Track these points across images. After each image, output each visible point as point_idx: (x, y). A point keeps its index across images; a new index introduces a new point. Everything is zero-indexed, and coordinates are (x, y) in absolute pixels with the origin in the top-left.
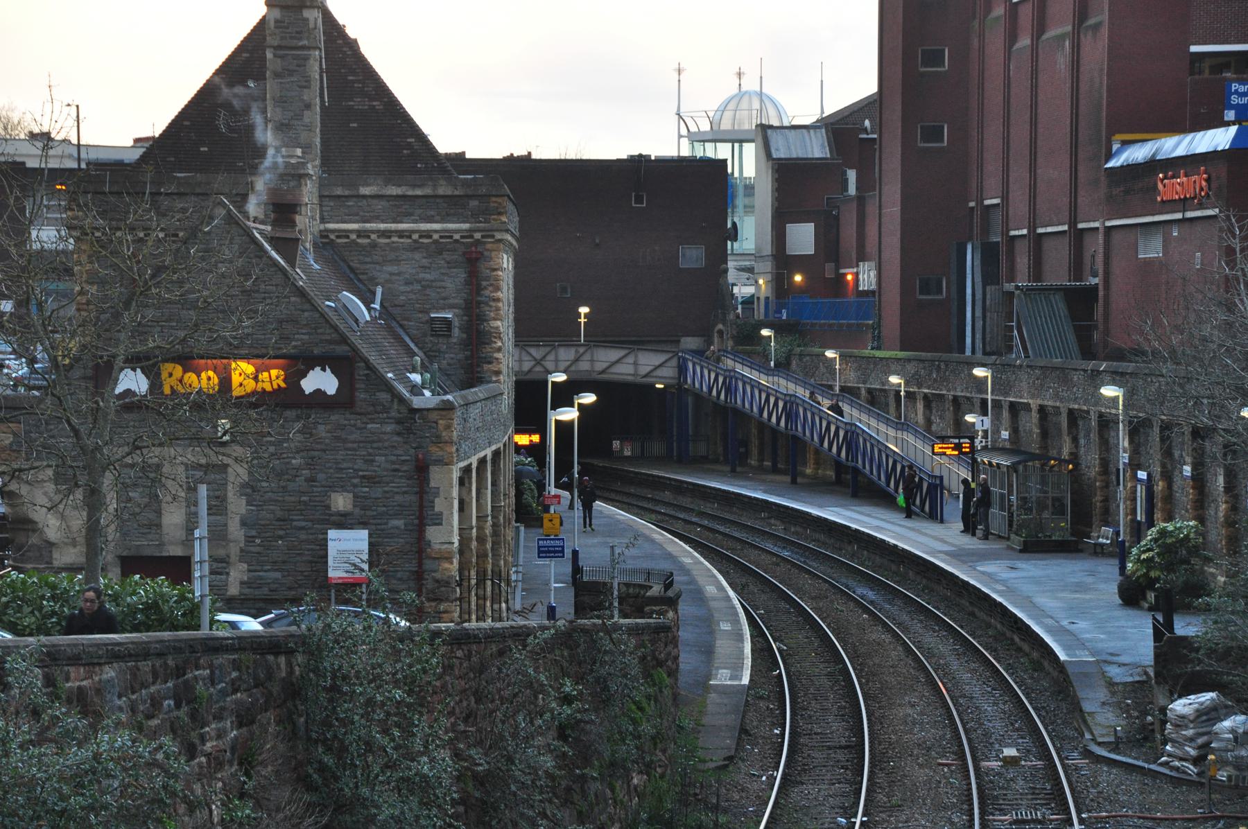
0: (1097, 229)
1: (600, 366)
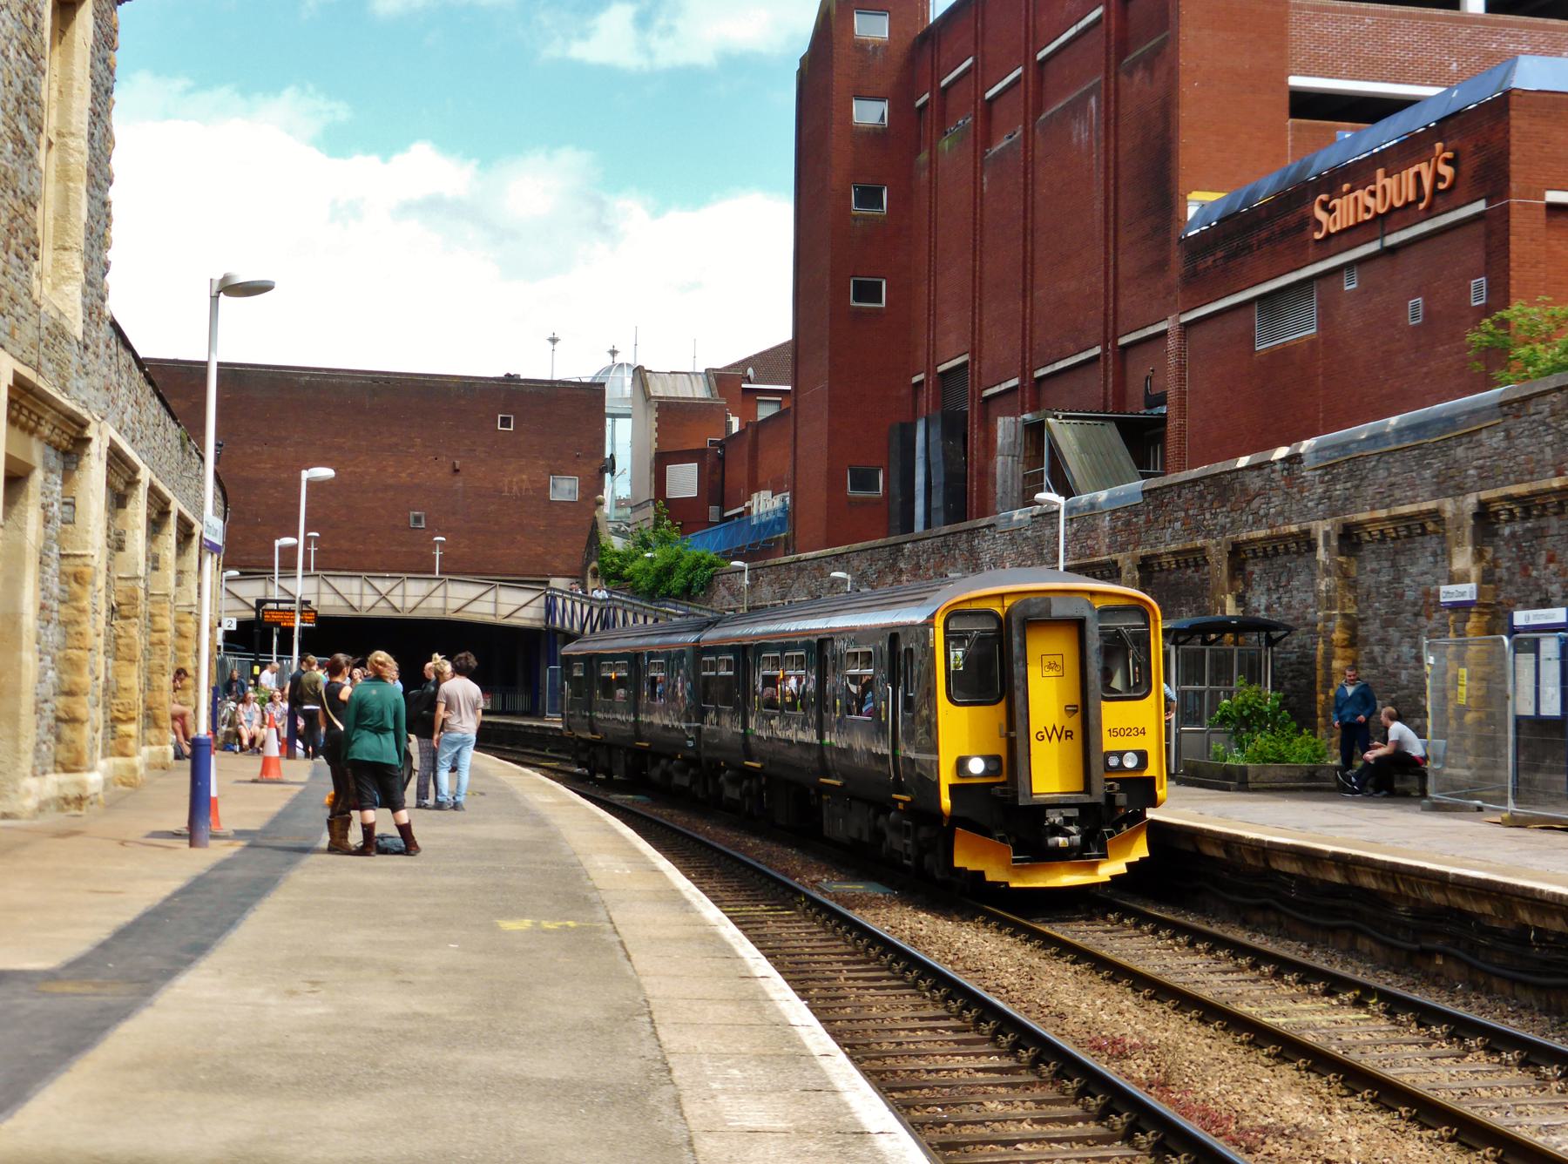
0: (1164, 333)
1: (454, 604)
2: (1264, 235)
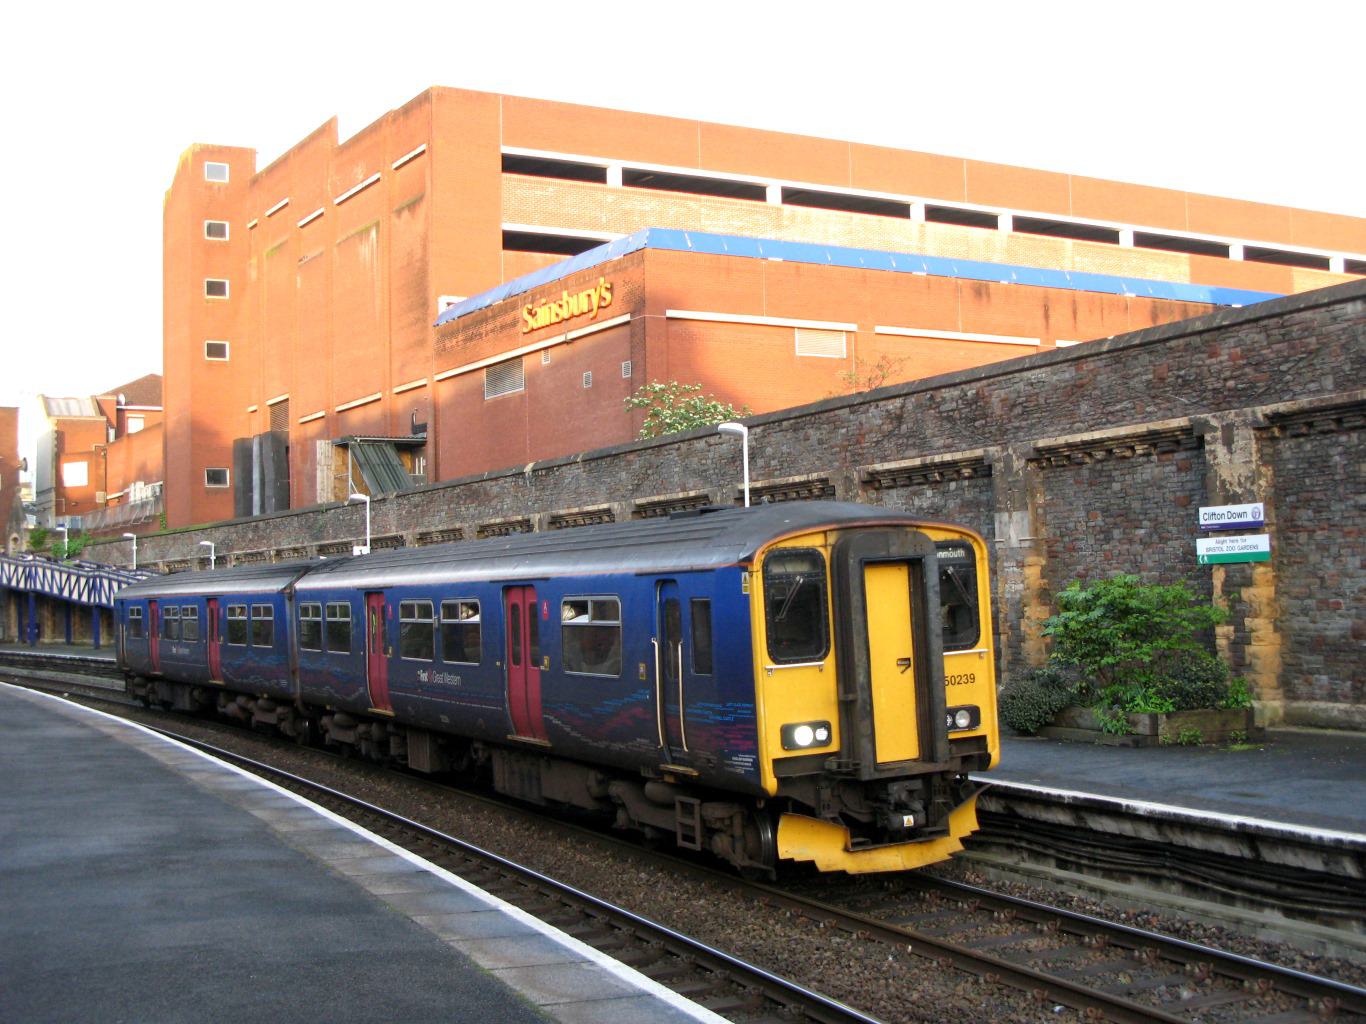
2: (490, 327)
